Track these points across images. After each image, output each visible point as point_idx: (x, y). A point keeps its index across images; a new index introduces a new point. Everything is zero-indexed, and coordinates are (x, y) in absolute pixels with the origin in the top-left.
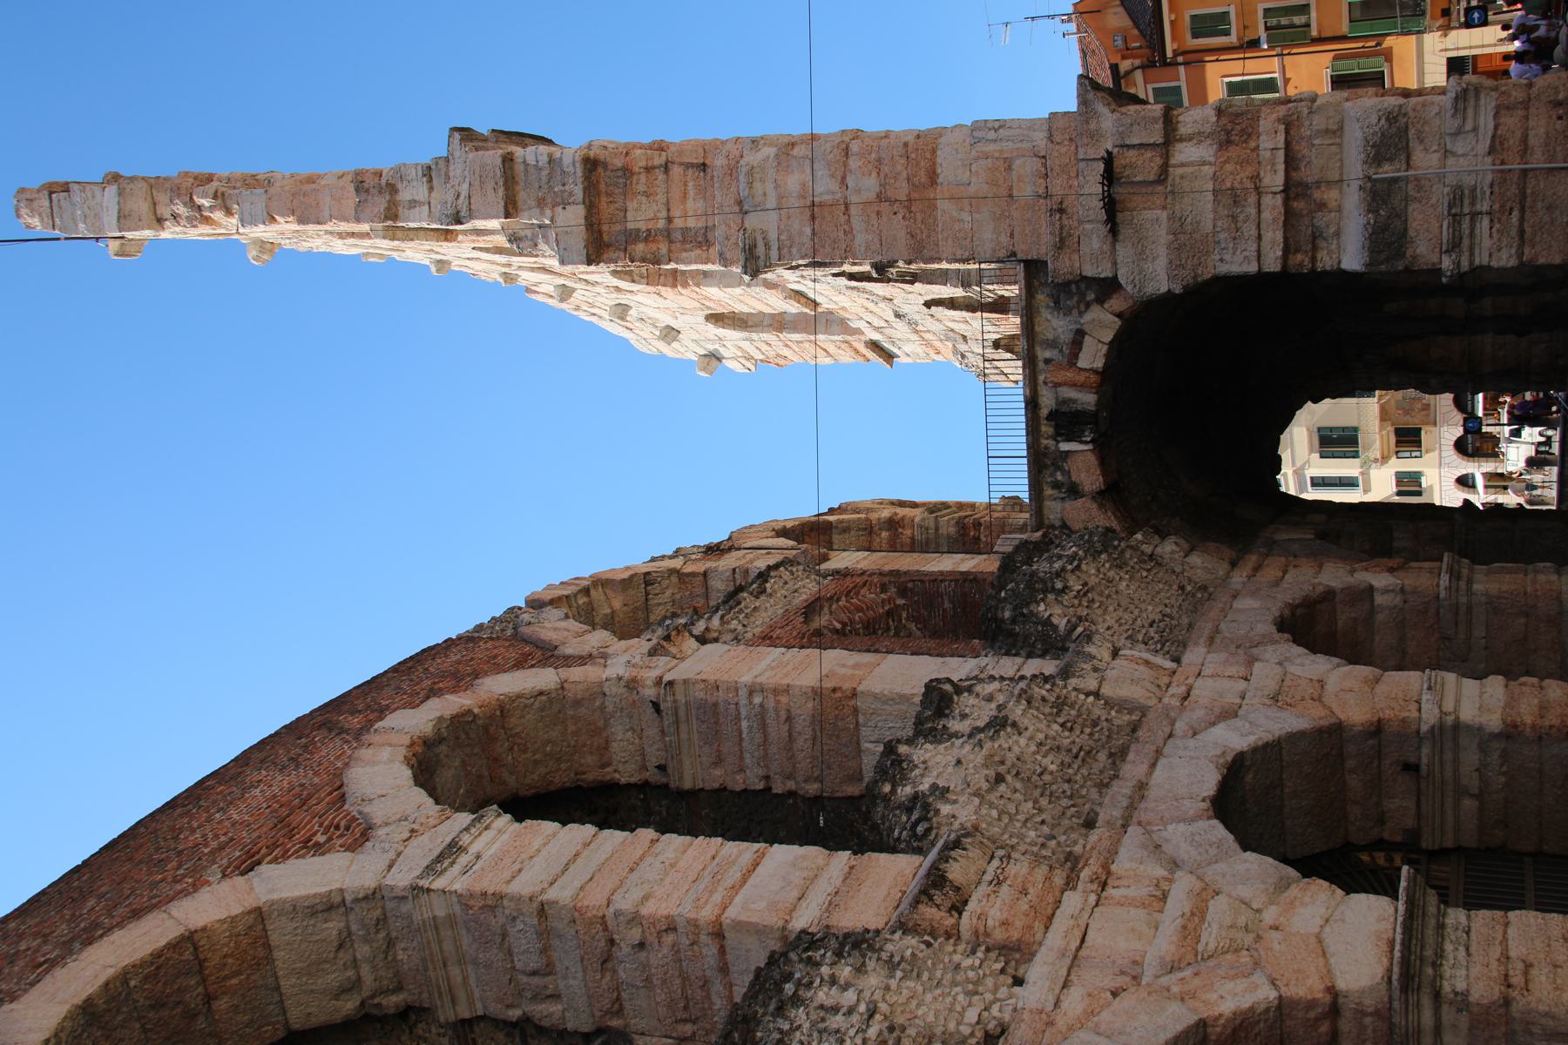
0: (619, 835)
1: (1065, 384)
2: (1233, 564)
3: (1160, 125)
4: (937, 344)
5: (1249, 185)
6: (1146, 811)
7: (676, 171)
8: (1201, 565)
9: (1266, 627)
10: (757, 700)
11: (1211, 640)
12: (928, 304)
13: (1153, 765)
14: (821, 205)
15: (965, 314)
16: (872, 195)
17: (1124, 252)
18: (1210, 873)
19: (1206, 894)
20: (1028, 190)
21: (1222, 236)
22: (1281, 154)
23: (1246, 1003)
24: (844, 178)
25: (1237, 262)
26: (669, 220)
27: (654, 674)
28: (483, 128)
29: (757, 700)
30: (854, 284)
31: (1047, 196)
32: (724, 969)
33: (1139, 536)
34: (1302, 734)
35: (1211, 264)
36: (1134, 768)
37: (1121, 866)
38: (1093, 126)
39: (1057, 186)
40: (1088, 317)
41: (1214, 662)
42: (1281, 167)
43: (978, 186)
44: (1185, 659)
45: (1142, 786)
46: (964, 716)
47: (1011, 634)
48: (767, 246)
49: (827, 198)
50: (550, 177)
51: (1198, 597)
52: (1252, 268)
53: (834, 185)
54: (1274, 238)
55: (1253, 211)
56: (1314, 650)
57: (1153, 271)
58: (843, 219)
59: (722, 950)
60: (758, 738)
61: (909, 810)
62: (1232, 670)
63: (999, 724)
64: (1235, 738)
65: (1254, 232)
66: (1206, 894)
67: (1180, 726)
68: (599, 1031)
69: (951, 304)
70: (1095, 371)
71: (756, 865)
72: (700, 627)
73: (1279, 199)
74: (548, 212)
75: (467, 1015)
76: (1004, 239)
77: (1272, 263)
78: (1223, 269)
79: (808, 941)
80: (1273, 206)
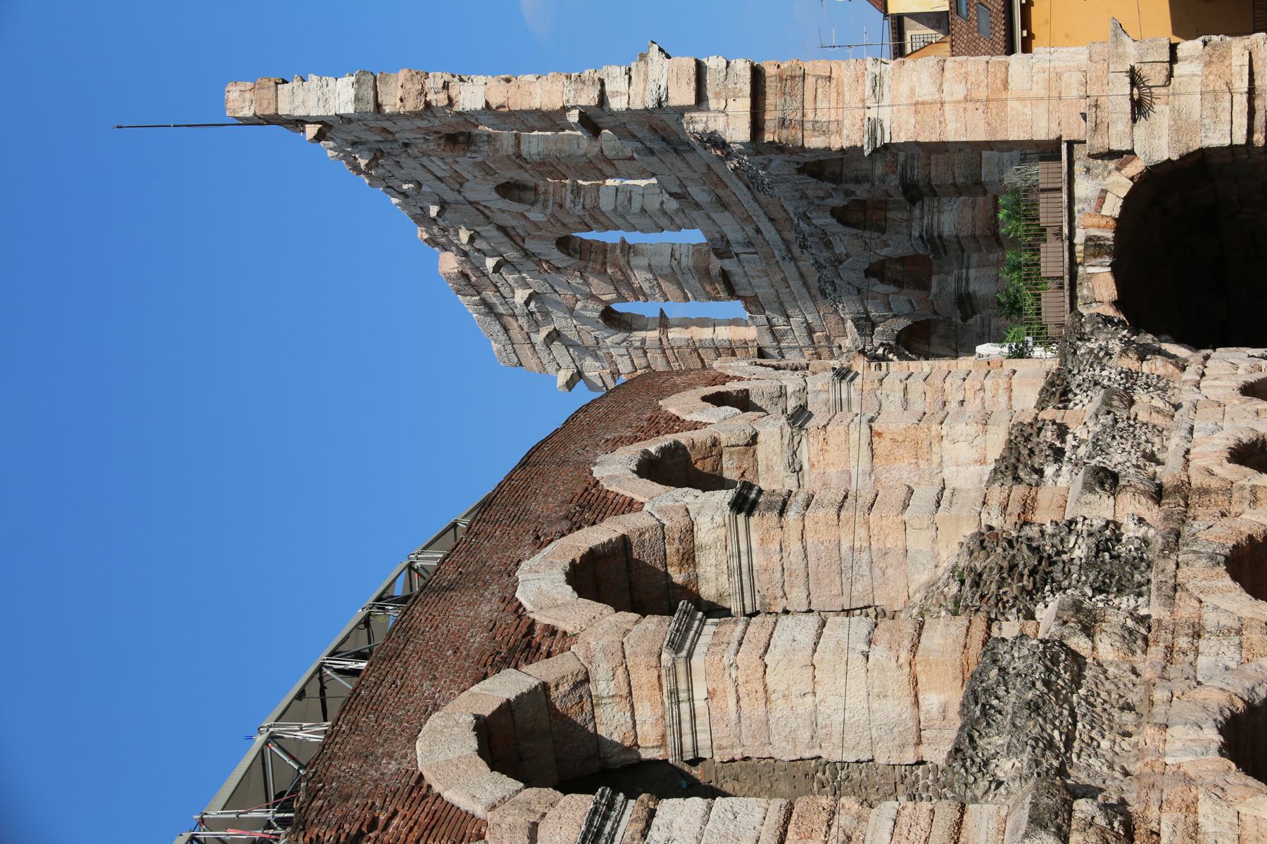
1: (1092, 226)
5: (1225, 87)
7: (810, 81)
14: (923, 103)
15: (892, 288)
16: (961, 97)
20: (1074, 93)
21: (1207, 121)
24: (941, 84)
25: (1217, 138)
35: (1198, 140)
38: (1120, 50)
39: (1094, 91)
40: (1110, 180)
42: (1246, 78)
43: (1039, 90)
48: (882, 130)
49: (929, 98)
52: (1227, 142)
53: (934, 89)
54: (1241, 122)
55: (1228, 105)
57: (1158, 143)
58: (938, 113)
73: (1245, 97)
76: (1054, 126)
77: (1240, 139)
80: (1241, 101)
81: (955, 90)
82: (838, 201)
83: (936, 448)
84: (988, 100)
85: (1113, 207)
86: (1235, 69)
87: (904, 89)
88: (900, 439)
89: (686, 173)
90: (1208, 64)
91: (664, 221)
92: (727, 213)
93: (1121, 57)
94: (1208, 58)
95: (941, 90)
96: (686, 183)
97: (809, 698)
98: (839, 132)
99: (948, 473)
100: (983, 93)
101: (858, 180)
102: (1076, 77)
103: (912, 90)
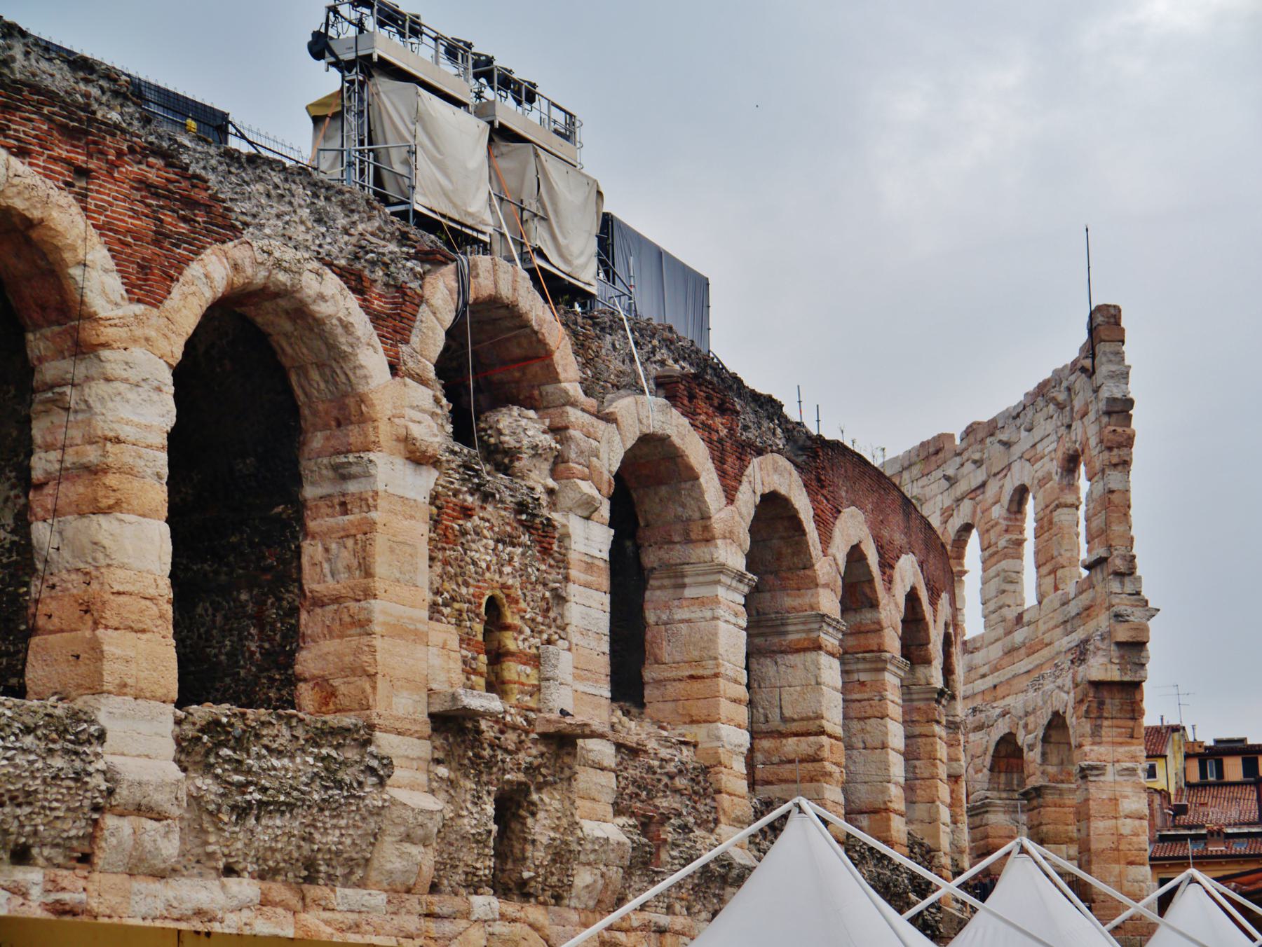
7: (1131, 723)
14: (1116, 805)
50: (1136, 664)
53: (1127, 812)
74: (1117, 661)
81: (1127, 826)
82: (1022, 739)
89: (1042, 627)
91: (992, 606)
92: (1001, 653)
95: (1127, 817)
96: (1032, 627)
97: (861, 745)
98: (1094, 744)
101: (1044, 754)
103: (1126, 797)
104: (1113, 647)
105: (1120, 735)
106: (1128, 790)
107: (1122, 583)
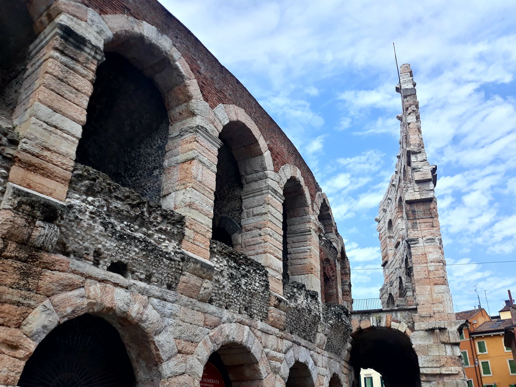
0: (281, 227)
2: (346, 362)
3: (454, 341)
4: (389, 279)
5: (442, 364)
6: (296, 346)
7: (431, 220)
8: (345, 353)
9: (333, 371)
10: (308, 251)
11: (330, 358)
12: (400, 278)
13: (304, 347)
17: (422, 333)
18: (284, 361)
19: (280, 361)
22: (451, 373)
23: (262, 372)
25: (421, 362)
26: (418, 219)
27: (311, 226)
28: (437, 172)
29: (308, 251)
30: (404, 260)
31: (434, 313)
32: (257, 254)
33: (351, 338)
34: (313, 382)
36: (303, 342)
37: (285, 341)
38: (453, 324)
39: (437, 316)
40: (404, 324)
41: (325, 359)
42: (447, 373)
44: (325, 352)
45: (299, 344)
46: (311, 301)
47: (328, 309)
48: (415, 244)
51: (338, 353)
52: (420, 365)
54: (429, 371)
55: (435, 366)
56: (330, 383)
57: (418, 341)
59: (261, 253)
60: (300, 251)
61: (292, 292)
62: (324, 364)
63: (310, 311)
64: (311, 365)
65: (430, 366)
66: (280, 361)
67: (312, 352)
68: (241, 226)
69: (401, 283)
70: (390, 326)
71: (278, 258)
72: (322, 235)
73: (439, 372)
75: (242, 198)
76: (422, 303)
77: (422, 371)
78: (419, 358)
79: (266, 274)
80: (437, 371)
83: (182, 187)
84: (429, 279)
85: (394, 325)
86: (450, 368)
87: (431, 250)
88: (188, 172)
90: (451, 358)
93: (450, 325)
94: (454, 358)
95: (431, 262)
99: (173, 194)
100: (431, 276)
102: (441, 309)
103: (430, 253)
104: (416, 185)
105: (426, 226)
106: (431, 250)
107: (417, 158)
